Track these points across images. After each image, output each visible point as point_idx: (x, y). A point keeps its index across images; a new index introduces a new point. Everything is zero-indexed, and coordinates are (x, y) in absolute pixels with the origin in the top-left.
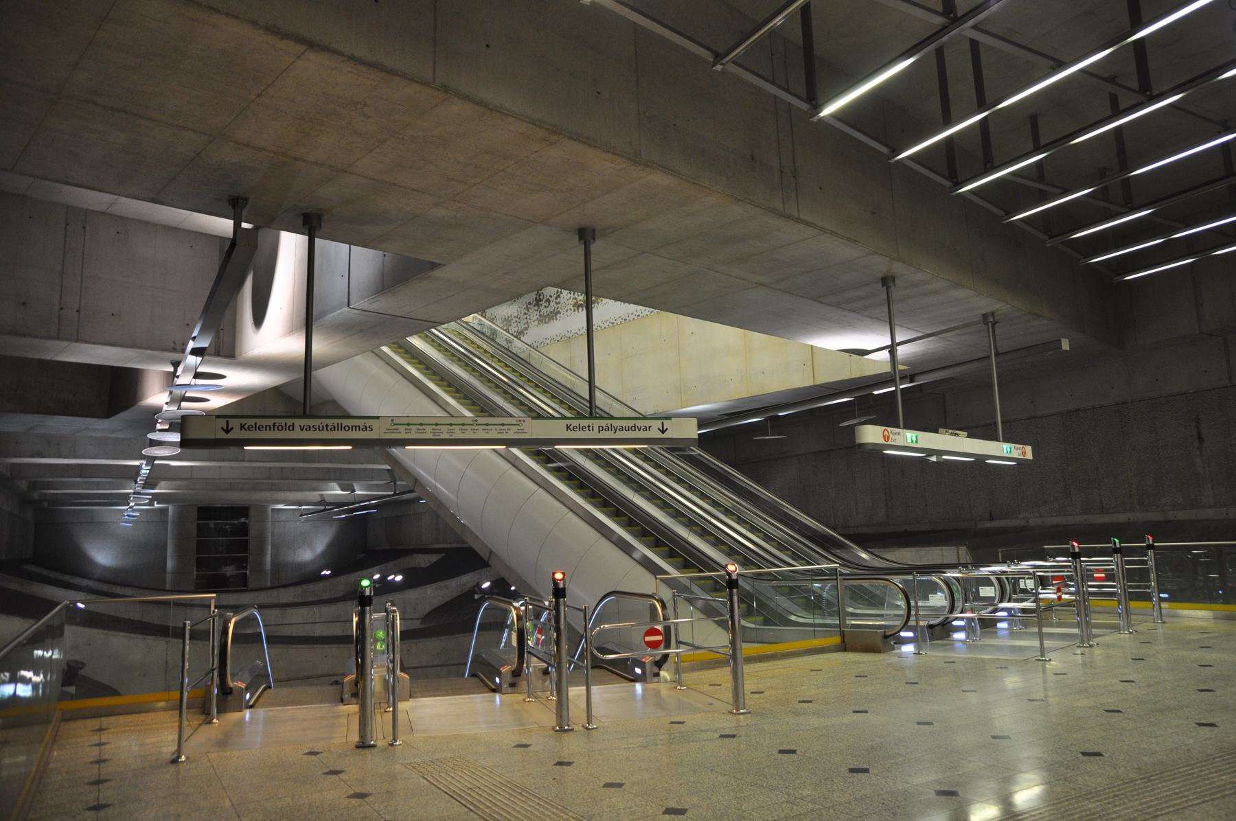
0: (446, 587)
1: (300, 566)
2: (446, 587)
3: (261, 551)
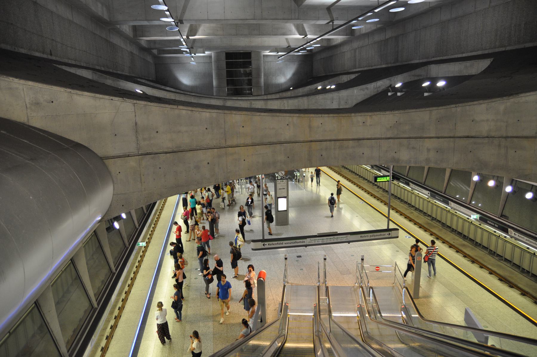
0: (367, 89)
1: (279, 85)
2: (367, 89)
3: (259, 76)
